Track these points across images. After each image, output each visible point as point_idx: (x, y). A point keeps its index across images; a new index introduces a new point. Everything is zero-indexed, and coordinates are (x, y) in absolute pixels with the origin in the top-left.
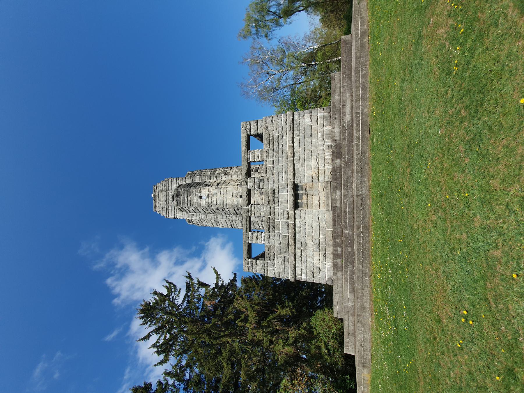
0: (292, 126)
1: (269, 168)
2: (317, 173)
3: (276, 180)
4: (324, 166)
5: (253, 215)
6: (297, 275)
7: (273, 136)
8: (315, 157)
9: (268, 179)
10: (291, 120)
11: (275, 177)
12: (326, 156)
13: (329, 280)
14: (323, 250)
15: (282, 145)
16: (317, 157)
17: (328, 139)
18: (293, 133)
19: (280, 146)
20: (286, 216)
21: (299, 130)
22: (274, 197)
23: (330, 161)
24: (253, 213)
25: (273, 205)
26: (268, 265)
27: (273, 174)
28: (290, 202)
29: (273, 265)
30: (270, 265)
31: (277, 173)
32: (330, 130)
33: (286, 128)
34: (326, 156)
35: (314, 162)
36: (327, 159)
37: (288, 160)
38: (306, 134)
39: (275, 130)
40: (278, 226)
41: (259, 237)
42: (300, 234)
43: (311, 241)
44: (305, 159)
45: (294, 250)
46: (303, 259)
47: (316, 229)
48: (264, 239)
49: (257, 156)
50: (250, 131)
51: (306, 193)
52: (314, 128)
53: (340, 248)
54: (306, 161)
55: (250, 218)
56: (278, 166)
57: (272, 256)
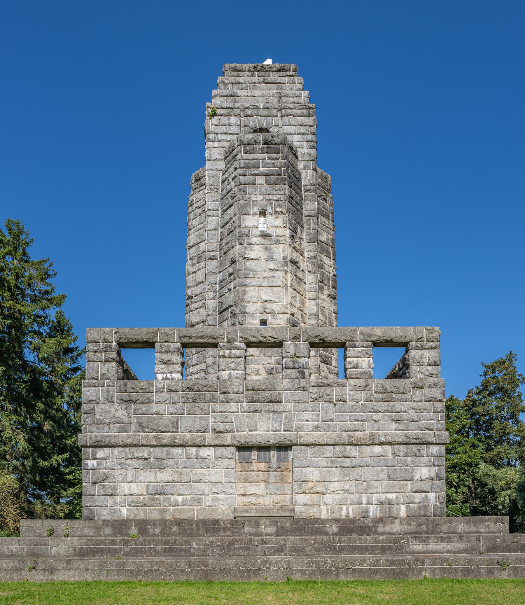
0: (417, 441)
1: (328, 392)
2: (314, 490)
3: (301, 406)
4: (327, 505)
5: (221, 354)
6: (94, 449)
7: (400, 400)
8: (347, 487)
9: (304, 389)
10: (430, 440)
11: (307, 405)
12: (348, 509)
13: (92, 512)
14: (153, 502)
15: (378, 420)
16: (345, 491)
17: (381, 511)
18: (401, 444)
19: (375, 416)
20: (221, 427)
21: (406, 455)
22: (262, 402)
23: (335, 516)
24: (227, 352)
25: (245, 399)
26: (108, 386)
27: (315, 400)
28: (252, 436)
29: (110, 397)
30: (108, 392)
31: (318, 409)
32: (399, 514)
33: (414, 429)
34: (348, 509)
35: (335, 486)
36: (341, 509)
37: (344, 434)
38: (396, 470)
39: (414, 404)
40: (198, 410)
41: (171, 368)
42: (182, 457)
43: (170, 479)
44: (343, 467)
45: (146, 444)
46: (129, 462)
47: (195, 488)
48: (166, 378)
49: (357, 364)
50: (417, 348)
51: (272, 470)
52: (407, 485)
53: (160, 532)
54: (338, 469)
55: (215, 346)
56: (332, 411)
57: (130, 396)
